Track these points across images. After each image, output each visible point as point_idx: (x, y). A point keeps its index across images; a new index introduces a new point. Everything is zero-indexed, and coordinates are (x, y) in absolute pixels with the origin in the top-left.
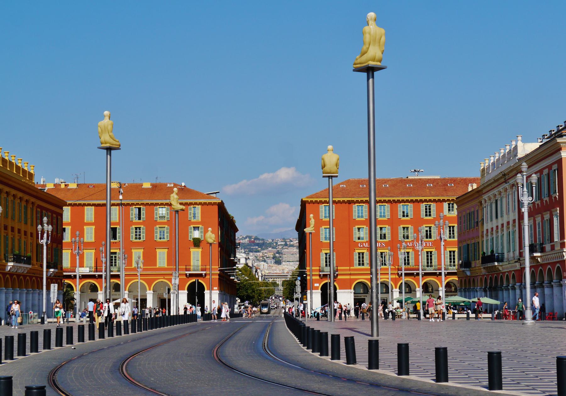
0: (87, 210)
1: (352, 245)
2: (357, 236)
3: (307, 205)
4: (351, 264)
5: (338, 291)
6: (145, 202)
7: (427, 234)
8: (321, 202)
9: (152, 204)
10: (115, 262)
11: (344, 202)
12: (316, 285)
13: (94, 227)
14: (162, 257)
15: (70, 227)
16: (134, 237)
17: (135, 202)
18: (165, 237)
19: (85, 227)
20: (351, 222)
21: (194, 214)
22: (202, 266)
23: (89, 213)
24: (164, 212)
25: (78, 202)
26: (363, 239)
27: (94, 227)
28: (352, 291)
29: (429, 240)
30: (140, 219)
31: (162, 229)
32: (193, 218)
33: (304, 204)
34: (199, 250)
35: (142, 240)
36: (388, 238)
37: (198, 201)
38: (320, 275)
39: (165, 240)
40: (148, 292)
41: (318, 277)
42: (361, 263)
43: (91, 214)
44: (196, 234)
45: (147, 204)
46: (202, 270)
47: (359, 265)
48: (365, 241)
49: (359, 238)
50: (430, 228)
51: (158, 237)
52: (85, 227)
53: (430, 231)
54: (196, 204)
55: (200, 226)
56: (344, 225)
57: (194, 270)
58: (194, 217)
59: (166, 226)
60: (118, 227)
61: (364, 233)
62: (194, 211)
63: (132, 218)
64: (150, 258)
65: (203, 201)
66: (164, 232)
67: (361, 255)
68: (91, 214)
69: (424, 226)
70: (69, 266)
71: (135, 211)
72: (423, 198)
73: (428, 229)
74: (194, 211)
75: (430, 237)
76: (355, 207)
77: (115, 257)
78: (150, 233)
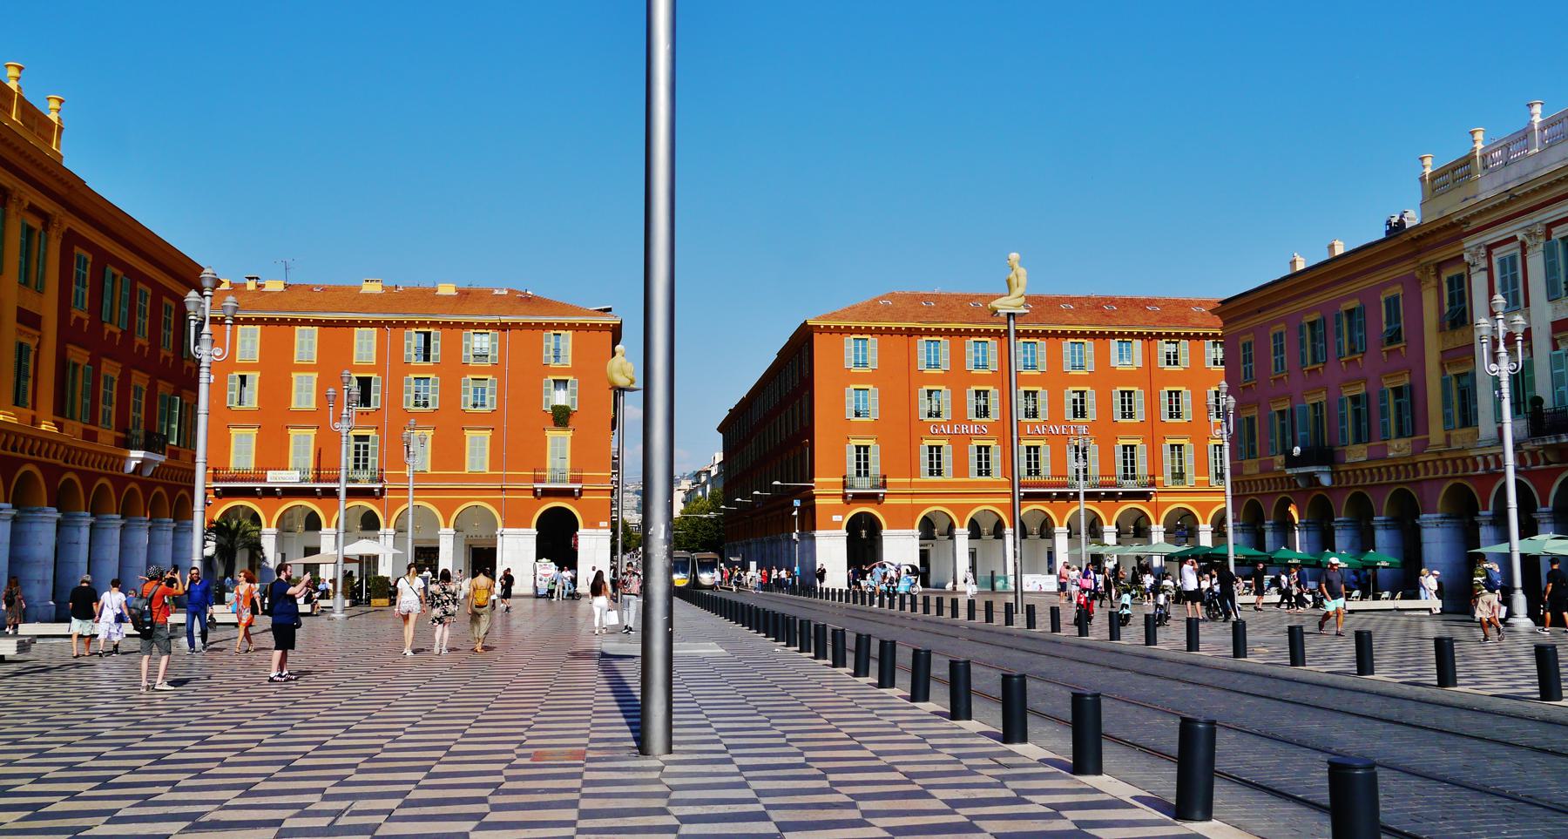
0: (302, 336)
1: (913, 429)
2: (927, 409)
3: (816, 335)
4: (913, 471)
5: (885, 532)
6: (441, 319)
7: (1075, 408)
9: (457, 325)
10: (366, 460)
11: (899, 329)
13: (315, 375)
14: (478, 450)
16: (412, 401)
17: (417, 318)
18: (487, 402)
19: (294, 375)
20: (912, 377)
21: (557, 350)
22: (572, 470)
23: (306, 343)
24: (485, 345)
25: (278, 315)
26: (938, 415)
27: (315, 375)
28: (917, 532)
29: (1079, 420)
30: (427, 358)
31: (480, 384)
34: (568, 434)
36: (995, 413)
37: (566, 320)
38: (844, 496)
39: (487, 409)
40: (443, 530)
41: (840, 501)
42: (935, 470)
43: (310, 344)
44: (561, 398)
45: (446, 324)
46: (572, 481)
47: (931, 473)
49: (930, 415)
50: (1082, 393)
51: (471, 402)
52: (294, 375)
53: (1082, 402)
54: (561, 326)
55: (570, 378)
56: (900, 383)
57: (553, 481)
58: (557, 357)
59: (490, 377)
60: (374, 376)
62: (557, 344)
64: (449, 452)
65: (577, 320)
66: (483, 391)
68: (310, 344)
69: (1071, 389)
70: (252, 466)
71: (414, 340)
72: (1069, 329)
73: (1077, 396)
74: (557, 344)
75: (1083, 416)
76: (922, 342)
77: (366, 447)
78: (451, 391)
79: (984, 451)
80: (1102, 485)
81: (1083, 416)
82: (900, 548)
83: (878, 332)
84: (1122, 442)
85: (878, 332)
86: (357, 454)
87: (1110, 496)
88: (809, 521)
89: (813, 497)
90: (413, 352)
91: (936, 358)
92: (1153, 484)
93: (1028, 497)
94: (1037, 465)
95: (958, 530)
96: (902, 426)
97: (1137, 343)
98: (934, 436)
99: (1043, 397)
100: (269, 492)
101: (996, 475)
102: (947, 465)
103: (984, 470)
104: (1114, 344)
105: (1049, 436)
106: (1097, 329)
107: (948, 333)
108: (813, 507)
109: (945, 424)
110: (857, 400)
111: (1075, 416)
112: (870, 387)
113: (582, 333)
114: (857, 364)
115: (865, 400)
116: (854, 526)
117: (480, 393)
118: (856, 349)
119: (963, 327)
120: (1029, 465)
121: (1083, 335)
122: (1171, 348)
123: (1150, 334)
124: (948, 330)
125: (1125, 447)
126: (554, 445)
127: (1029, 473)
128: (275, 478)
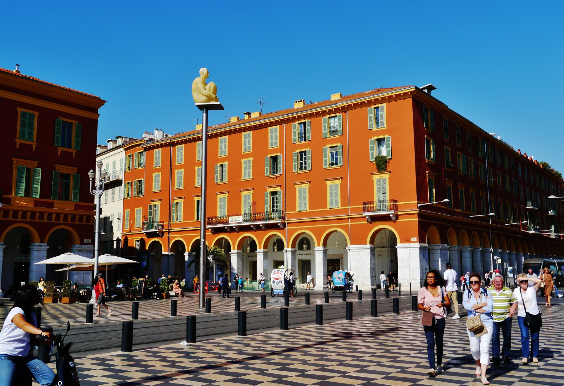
9: (317, 114)
13: (251, 159)
15: (227, 163)
19: (243, 161)
21: (377, 119)
30: (305, 140)
32: (374, 126)
34: (387, 176)
35: (308, 169)
40: (317, 248)
43: (249, 141)
44: (384, 151)
45: (312, 114)
46: (391, 209)
54: (377, 101)
57: (378, 210)
58: (377, 123)
59: (338, 144)
60: (278, 154)
63: (295, 139)
64: (318, 197)
65: (386, 95)
66: (336, 154)
74: (378, 115)
77: (277, 198)
78: (318, 156)
86: (273, 203)
90: (297, 137)
100: (232, 230)
113: (393, 103)
117: (334, 156)
126: (378, 184)
128: (236, 221)
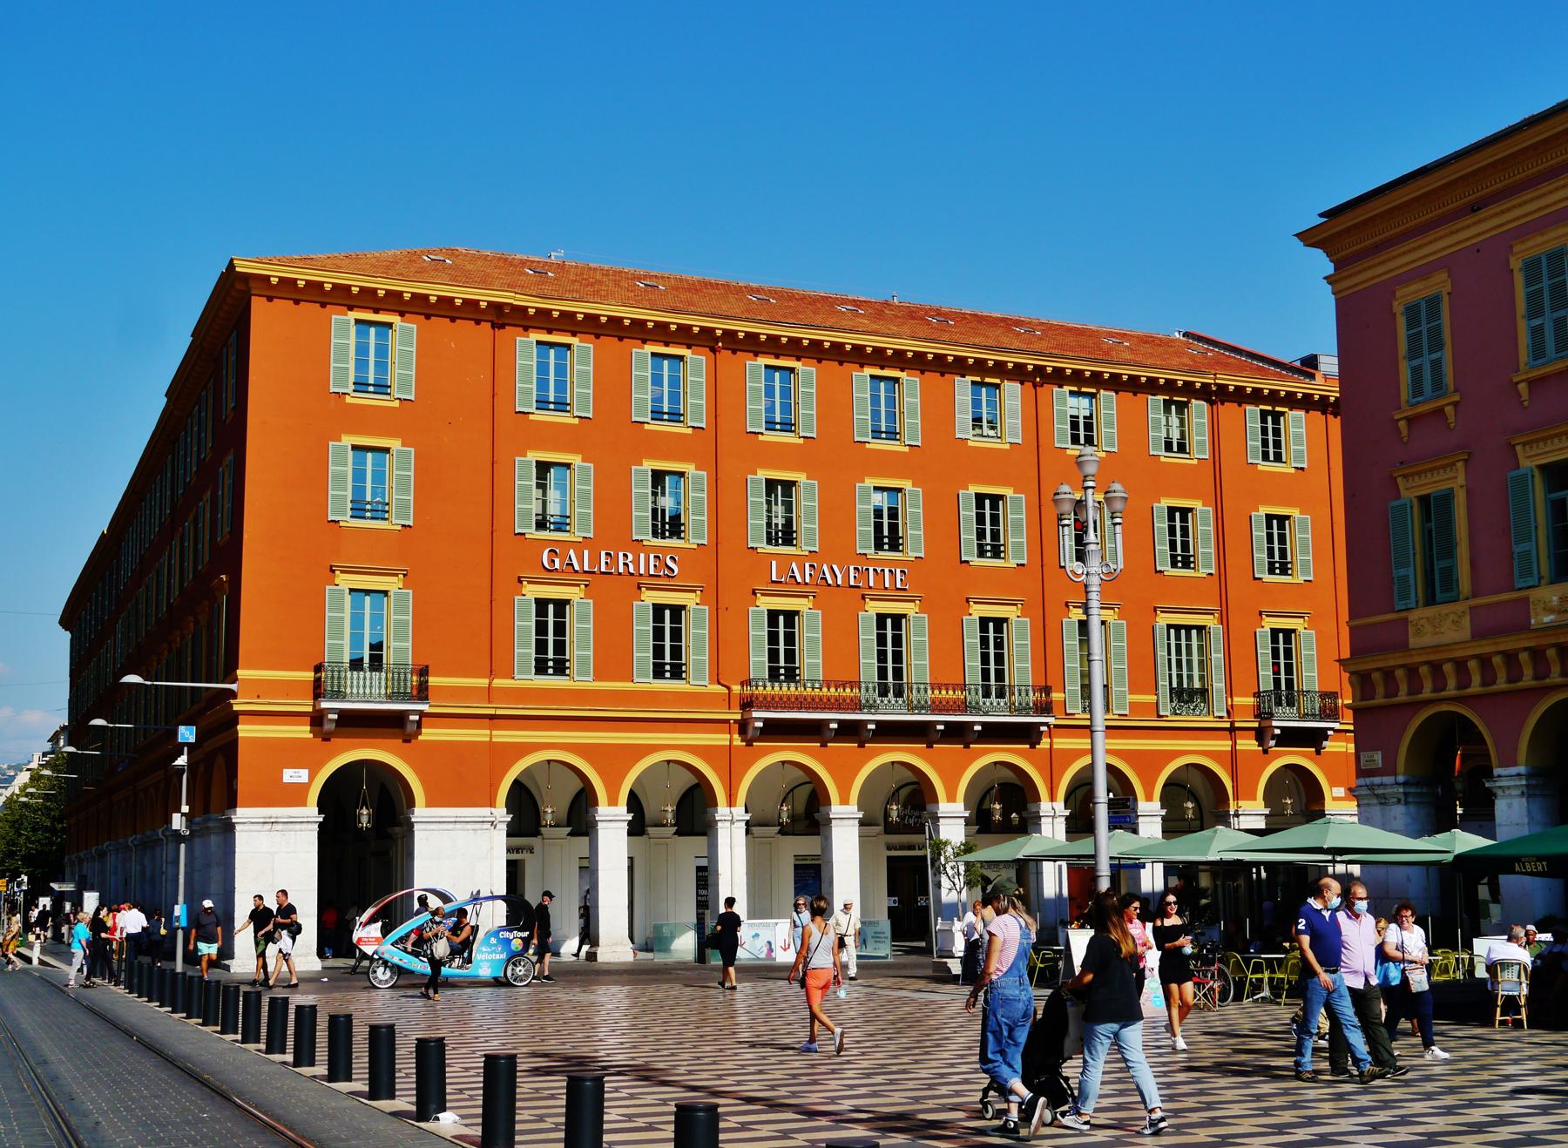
1: (501, 557)
2: (536, 507)
4: (498, 663)
5: (421, 812)
8: (343, 297)
11: (471, 304)
12: (293, 776)
20: (500, 427)
28: (501, 813)
33: (230, 309)
38: (317, 719)
41: (303, 731)
42: (552, 660)
47: (541, 668)
48: (576, 535)
49: (541, 525)
56: (469, 446)
61: (577, 494)
67: (552, 614)
79: (668, 618)
80: (937, 707)
81: (894, 547)
82: (457, 854)
83: (418, 307)
84: (978, 611)
85: (418, 307)
87: (957, 733)
88: (219, 784)
89: (234, 719)
91: (561, 387)
92: (1045, 708)
93: (775, 730)
94: (790, 656)
95: (603, 810)
96: (466, 553)
97: (1012, 391)
98: (550, 575)
99: (807, 502)
101: (698, 680)
102: (580, 648)
103: (669, 665)
104: (963, 386)
105: (819, 589)
106: (931, 349)
107: (591, 326)
108: (231, 748)
109: (578, 546)
110: (359, 475)
111: (879, 546)
112: (395, 444)
114: (361, 386)
115: (379, 477)
116: (337, 798)
118: (362, 349)
119: (628, 313)
120: (773, 656)
121: (899, 359)
122: (1081, 407)
123: (1039, 370)
124: (592, 319)
125: (984, 622)
127: (774, 675)
